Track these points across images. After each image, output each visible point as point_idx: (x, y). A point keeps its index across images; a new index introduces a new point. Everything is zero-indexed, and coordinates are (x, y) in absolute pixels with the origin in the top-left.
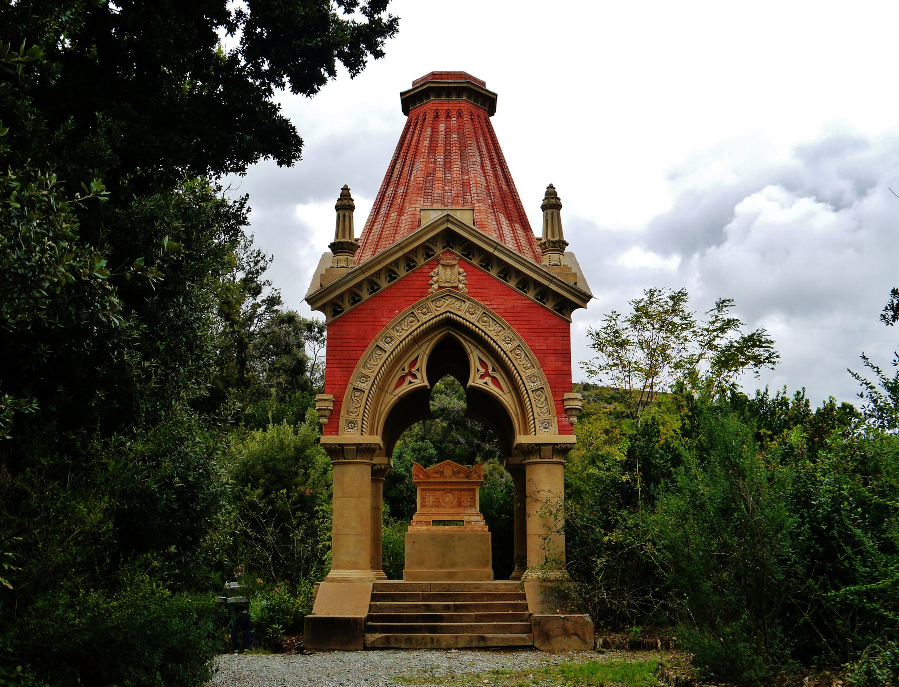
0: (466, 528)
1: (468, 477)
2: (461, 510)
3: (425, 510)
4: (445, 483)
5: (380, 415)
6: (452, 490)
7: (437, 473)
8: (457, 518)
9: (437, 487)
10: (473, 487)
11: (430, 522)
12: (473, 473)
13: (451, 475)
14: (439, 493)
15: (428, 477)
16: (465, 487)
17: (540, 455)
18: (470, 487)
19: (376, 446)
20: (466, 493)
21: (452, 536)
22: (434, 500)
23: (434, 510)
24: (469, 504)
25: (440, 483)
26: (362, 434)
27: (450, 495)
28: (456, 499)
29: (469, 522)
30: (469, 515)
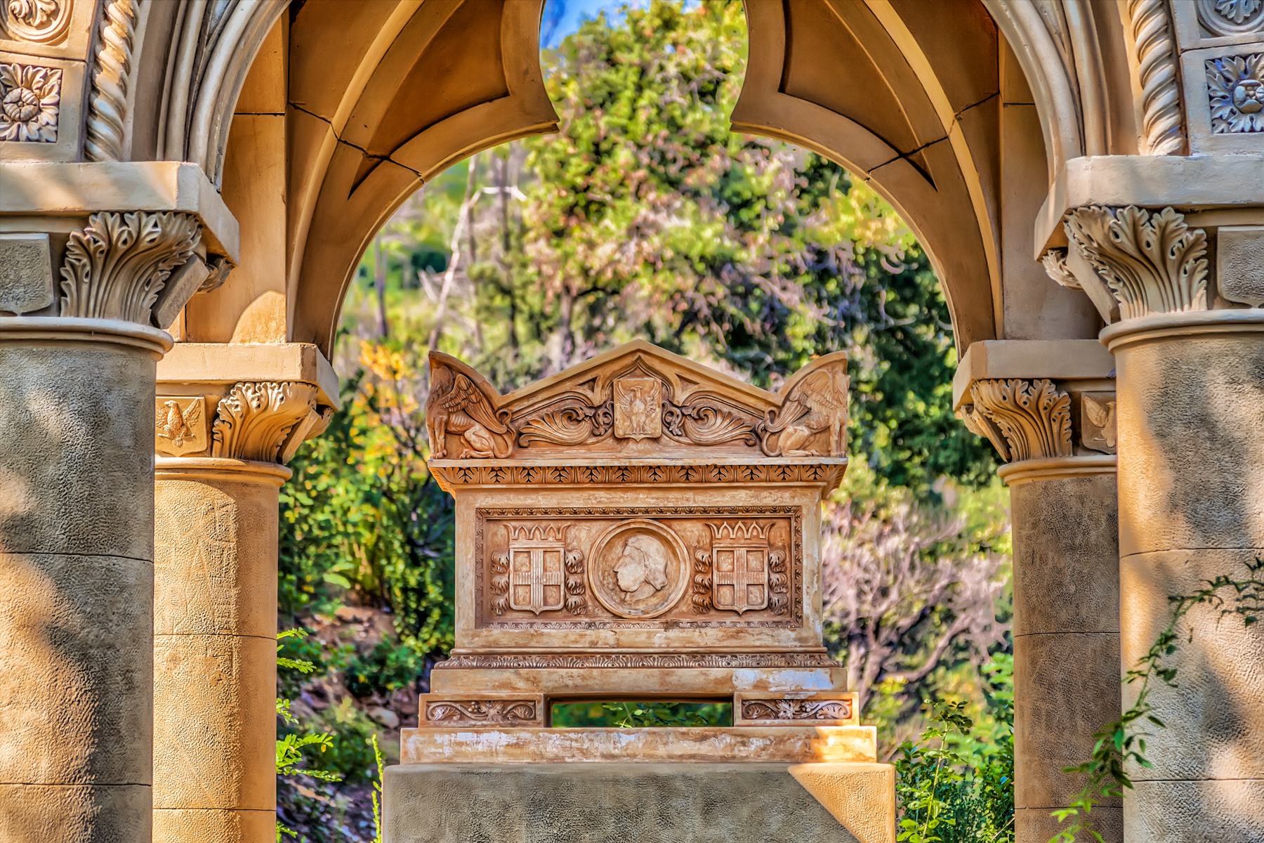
0: (744, 739)
1: (755, 438)
2: (710, 636)
3: (500, 635)
4: (624, 476)
5: (208, 39)
6: (665, 517)
7: (571, 416)
8: (690, 678)
9: (576, 500)
10: (785, 499)
11: (528, 704)
12: (790, 412)
13: (655, 427)
14: (585, 537)
15: (520, 440)
16: (741, 498)
17: (1211, 278)
18: (769, 499)
19: (176, 228)
20: (754, 530)
21: (662, 785)
22: (557, 576)
23: (557, 635)
24: (758, 597)
25: (593, 476)
26: (87, 155)
27: (651, 546)
28: (686, 570)
29: (767, 707)
30: (762, 658)
